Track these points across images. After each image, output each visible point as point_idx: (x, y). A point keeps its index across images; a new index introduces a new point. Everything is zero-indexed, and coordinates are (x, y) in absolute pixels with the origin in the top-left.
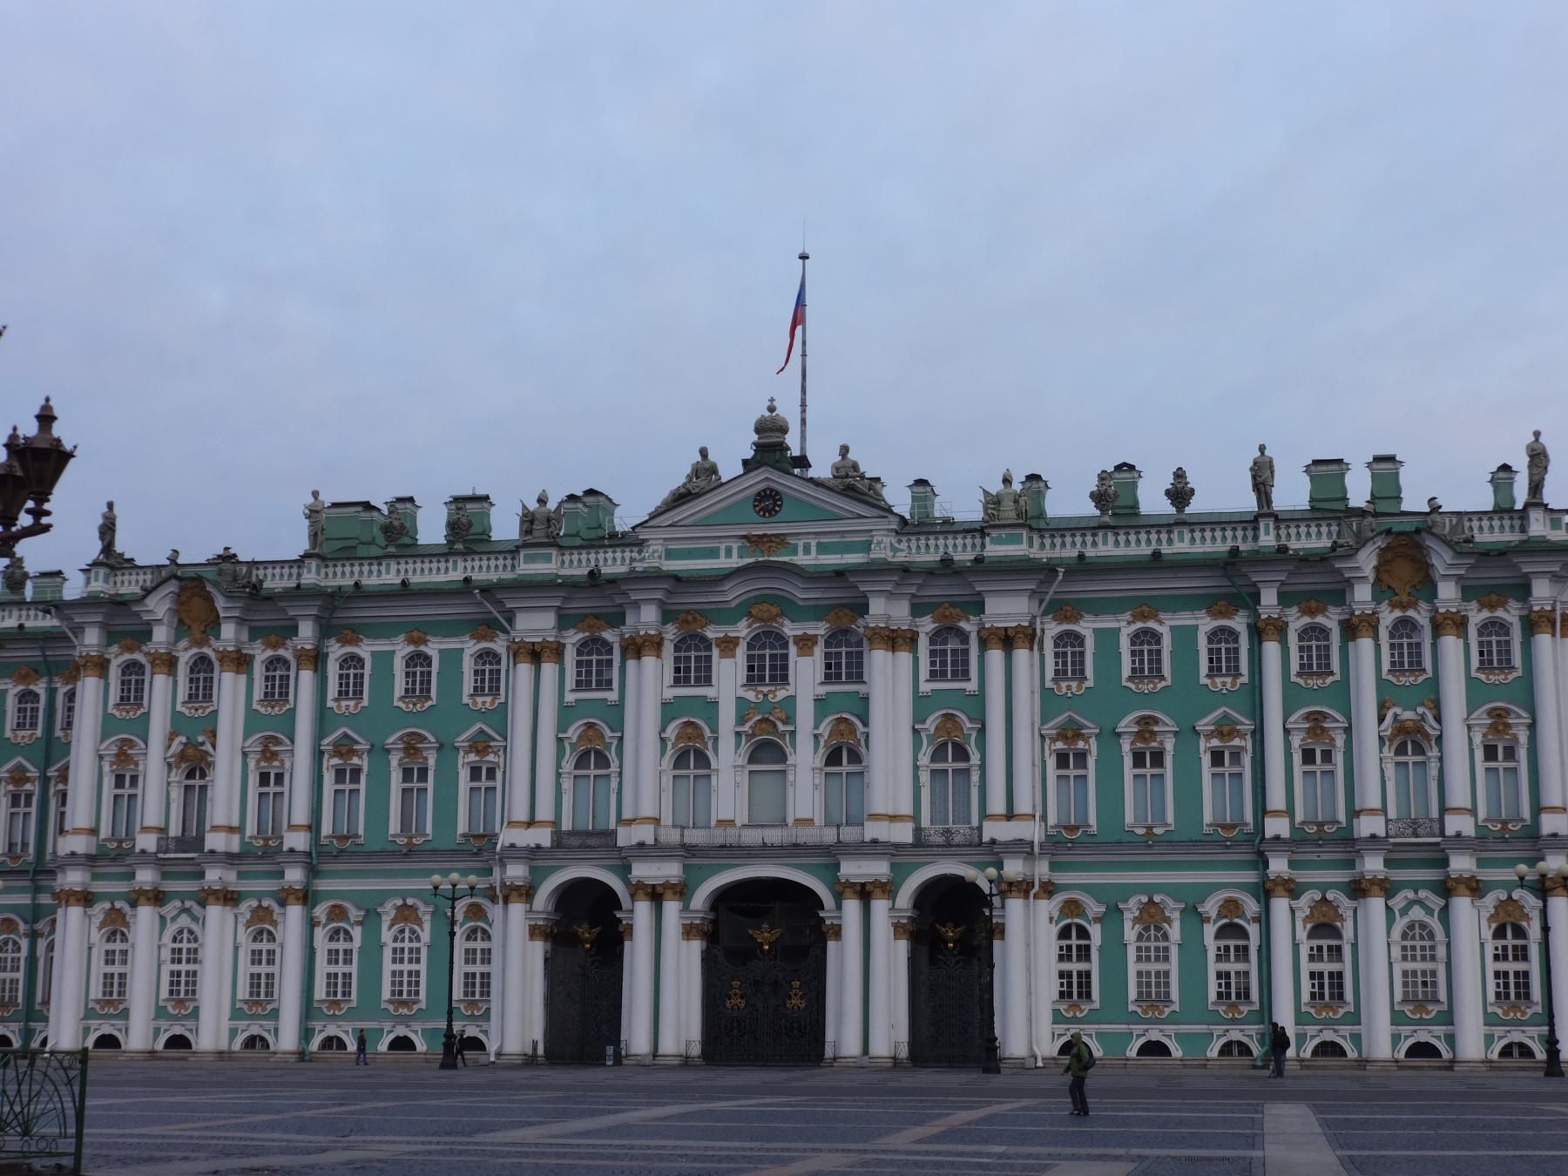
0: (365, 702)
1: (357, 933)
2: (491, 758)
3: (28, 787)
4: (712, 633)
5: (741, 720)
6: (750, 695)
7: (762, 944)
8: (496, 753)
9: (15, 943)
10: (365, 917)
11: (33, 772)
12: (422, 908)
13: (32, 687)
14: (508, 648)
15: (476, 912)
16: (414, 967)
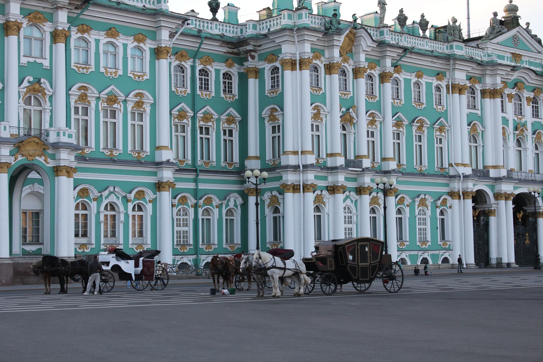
0: (403, 102)
1: (407, 210)
2: (443, 134)
3: (185, 121)
4: (507, 91)
5: (516, 129)
6: (516, 119)
7: (518, 219)
8: (445, 132)
9: (184, 210)
10: (411, 203)
11: (190, 113)
12: (429, 200)
13: (183, 63)
14: (448, 86)
15: (444, 202)
16: (424, 227)
